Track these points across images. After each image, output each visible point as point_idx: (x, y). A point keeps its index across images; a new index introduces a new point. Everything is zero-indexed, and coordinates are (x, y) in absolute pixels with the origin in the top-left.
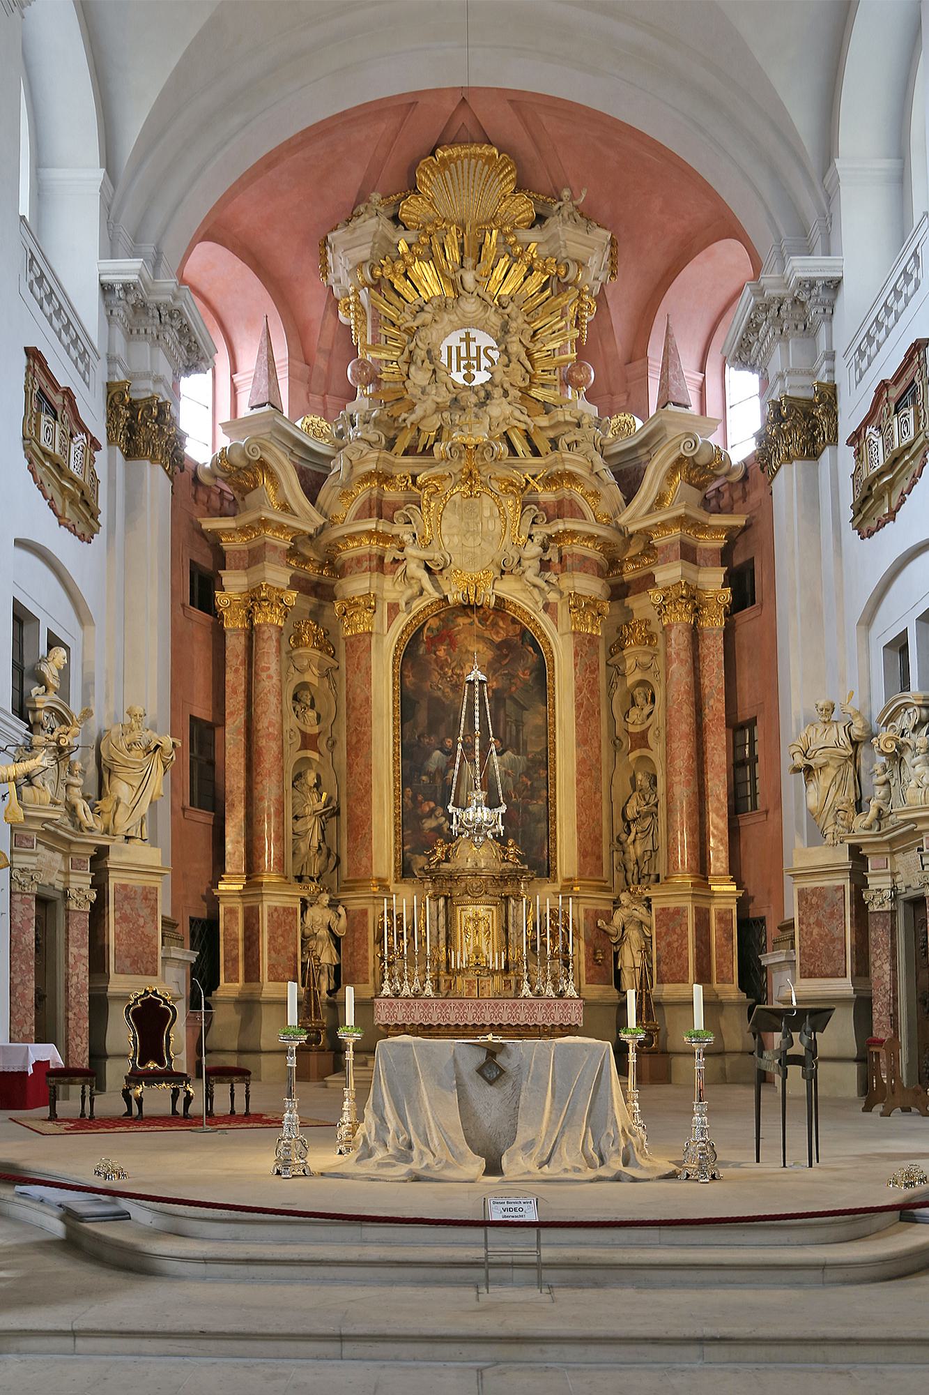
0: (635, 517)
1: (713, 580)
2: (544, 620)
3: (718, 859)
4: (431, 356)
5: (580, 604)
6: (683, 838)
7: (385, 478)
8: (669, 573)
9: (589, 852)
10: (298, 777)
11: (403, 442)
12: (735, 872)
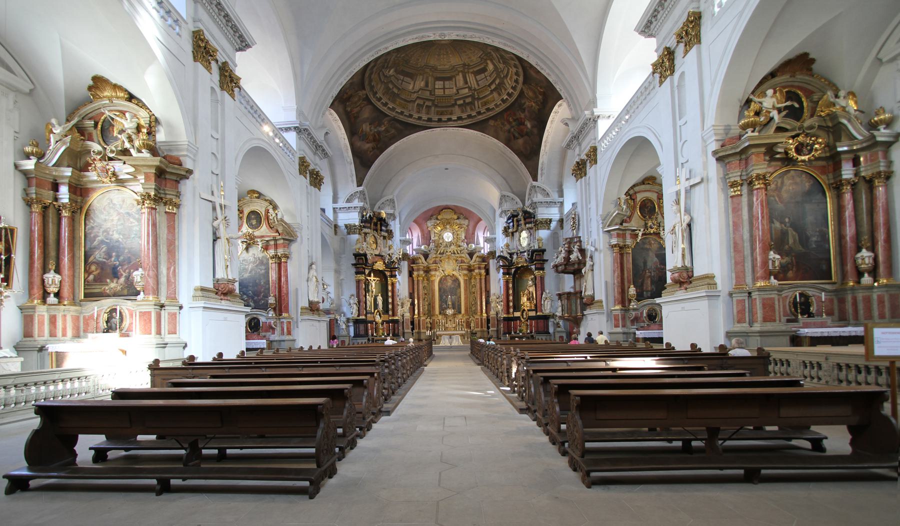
0: (472, 263)
1: (483, 271)
2: (459, 277)
3: (484, 311)
4: (443, 238)
5: (465, 275)
6: (479, 308)
7: (437, 257)
8: (477, 271)
9: (466, 310)
10: (424, 299)
11: (439, 253)
12: (487, 312)
